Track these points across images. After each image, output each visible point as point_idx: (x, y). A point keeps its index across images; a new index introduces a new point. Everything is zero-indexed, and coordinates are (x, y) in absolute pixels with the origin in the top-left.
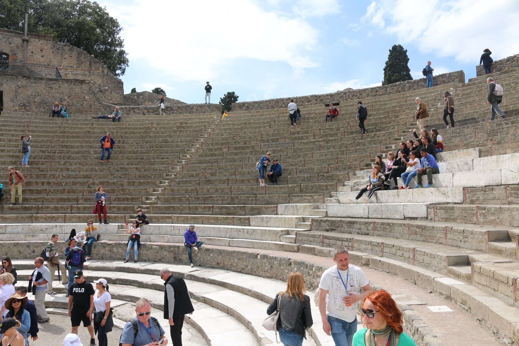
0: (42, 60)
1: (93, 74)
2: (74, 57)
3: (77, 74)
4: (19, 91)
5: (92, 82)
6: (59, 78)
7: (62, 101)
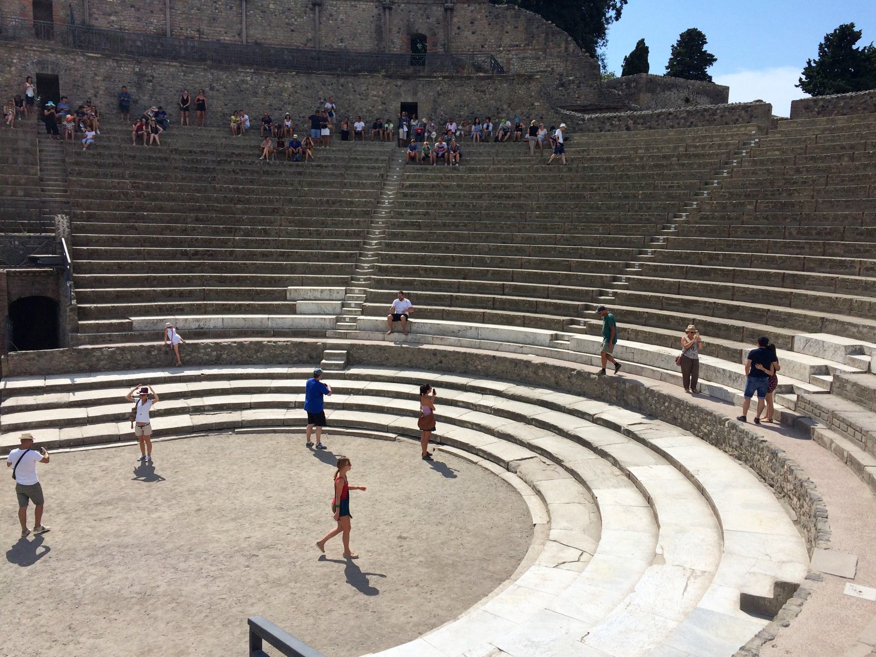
0: (473, 38)
1: (551, 55)
2: (521, 28)
3: (524, 58)
5: (549, 69)
7: (498, 113)
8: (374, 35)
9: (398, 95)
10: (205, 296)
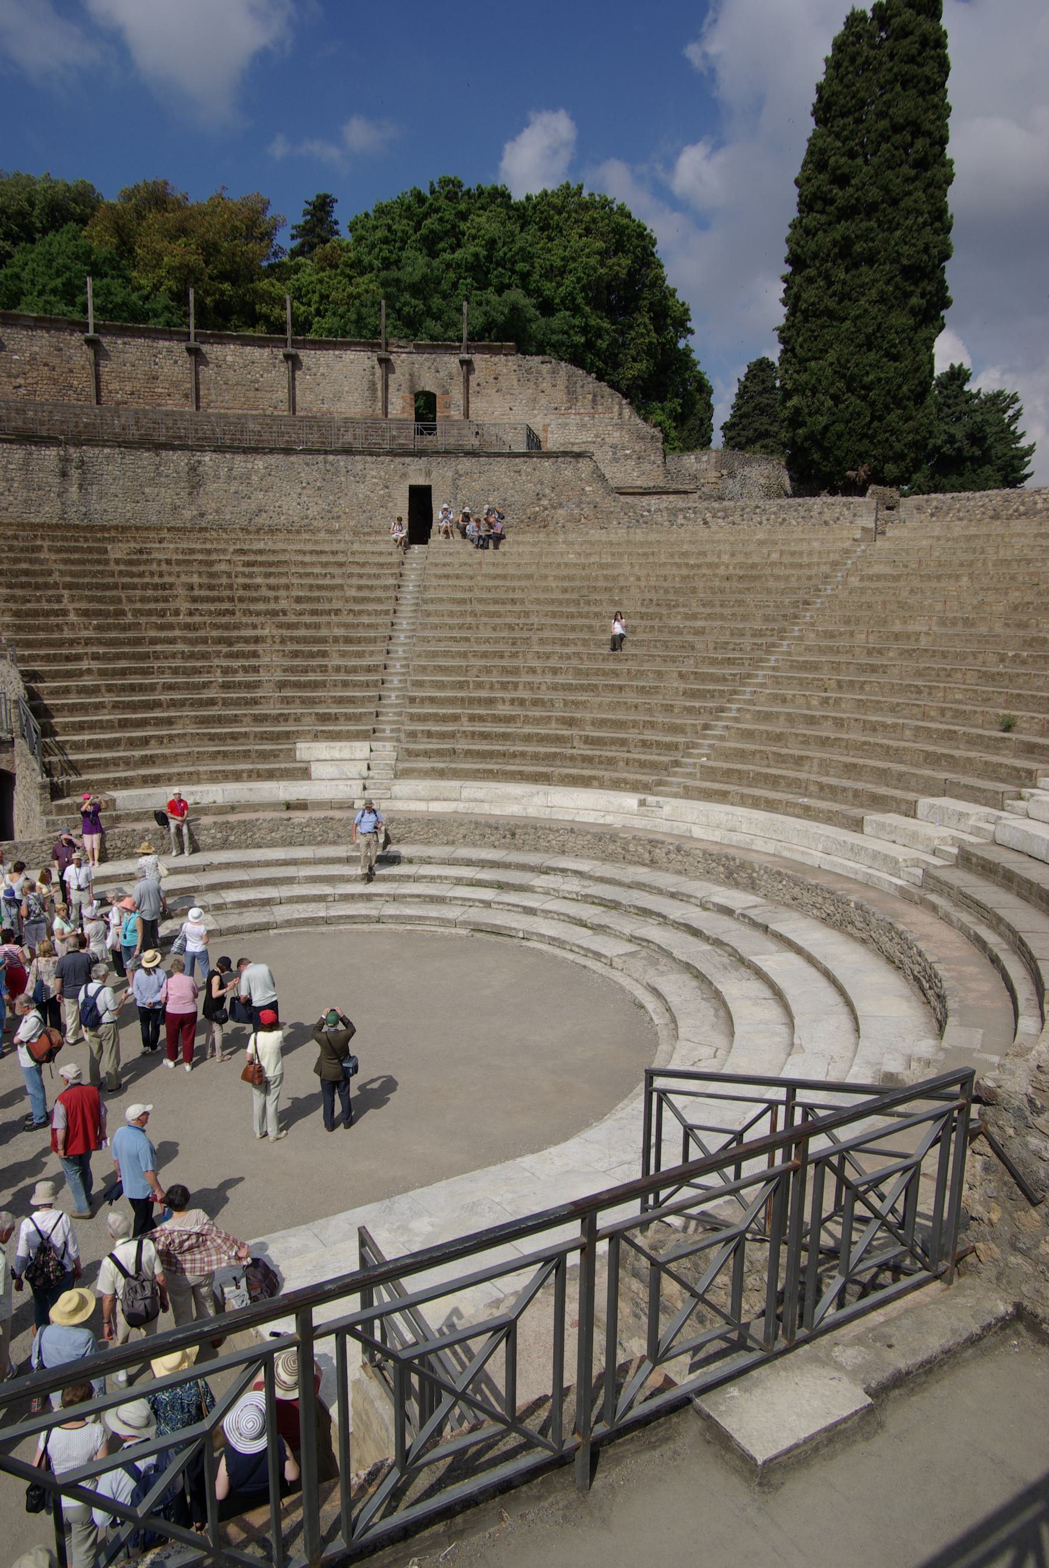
4: (460, 483)
6: (534, 446)
8: (367, 394)
9: (404, 475)
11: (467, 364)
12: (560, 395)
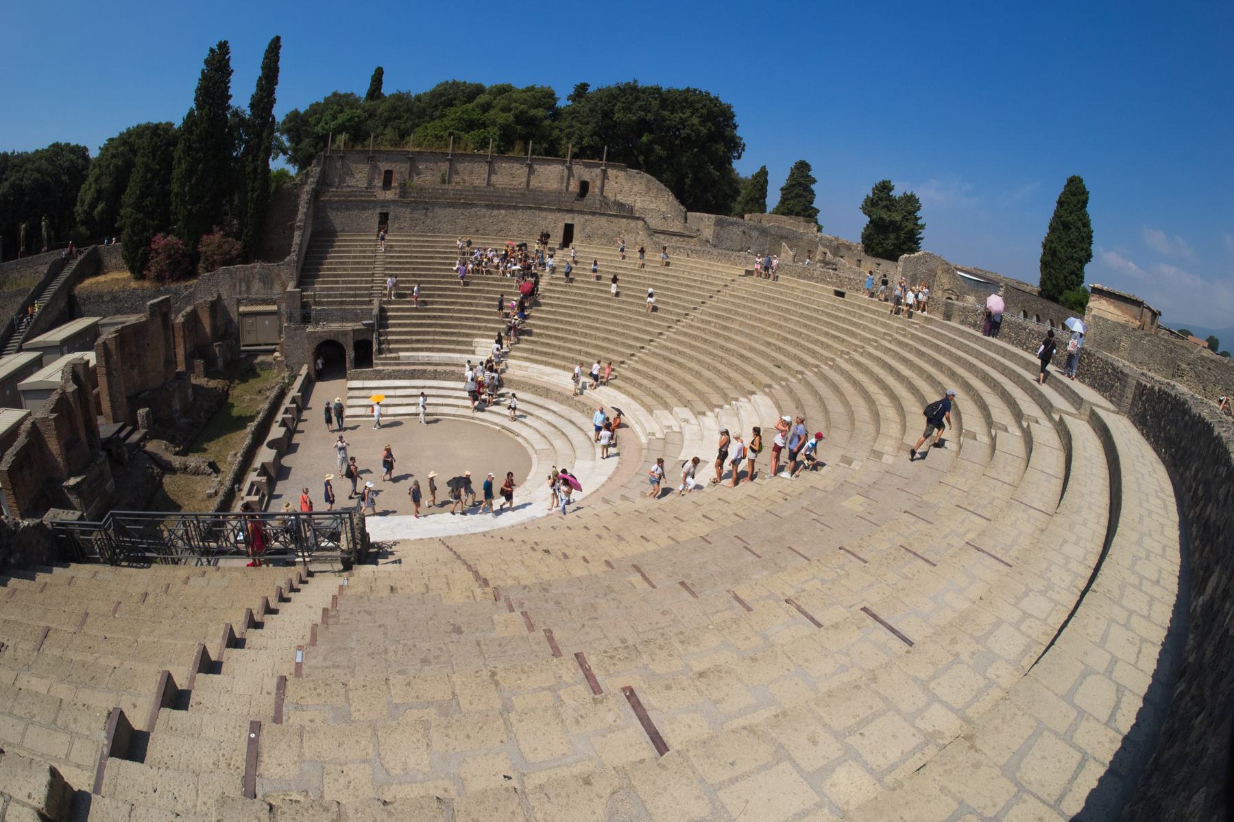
10: (435, 342)
11: (604, 172)
12: (642, 188)
